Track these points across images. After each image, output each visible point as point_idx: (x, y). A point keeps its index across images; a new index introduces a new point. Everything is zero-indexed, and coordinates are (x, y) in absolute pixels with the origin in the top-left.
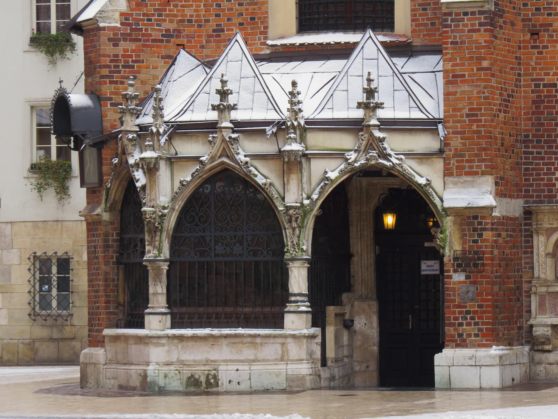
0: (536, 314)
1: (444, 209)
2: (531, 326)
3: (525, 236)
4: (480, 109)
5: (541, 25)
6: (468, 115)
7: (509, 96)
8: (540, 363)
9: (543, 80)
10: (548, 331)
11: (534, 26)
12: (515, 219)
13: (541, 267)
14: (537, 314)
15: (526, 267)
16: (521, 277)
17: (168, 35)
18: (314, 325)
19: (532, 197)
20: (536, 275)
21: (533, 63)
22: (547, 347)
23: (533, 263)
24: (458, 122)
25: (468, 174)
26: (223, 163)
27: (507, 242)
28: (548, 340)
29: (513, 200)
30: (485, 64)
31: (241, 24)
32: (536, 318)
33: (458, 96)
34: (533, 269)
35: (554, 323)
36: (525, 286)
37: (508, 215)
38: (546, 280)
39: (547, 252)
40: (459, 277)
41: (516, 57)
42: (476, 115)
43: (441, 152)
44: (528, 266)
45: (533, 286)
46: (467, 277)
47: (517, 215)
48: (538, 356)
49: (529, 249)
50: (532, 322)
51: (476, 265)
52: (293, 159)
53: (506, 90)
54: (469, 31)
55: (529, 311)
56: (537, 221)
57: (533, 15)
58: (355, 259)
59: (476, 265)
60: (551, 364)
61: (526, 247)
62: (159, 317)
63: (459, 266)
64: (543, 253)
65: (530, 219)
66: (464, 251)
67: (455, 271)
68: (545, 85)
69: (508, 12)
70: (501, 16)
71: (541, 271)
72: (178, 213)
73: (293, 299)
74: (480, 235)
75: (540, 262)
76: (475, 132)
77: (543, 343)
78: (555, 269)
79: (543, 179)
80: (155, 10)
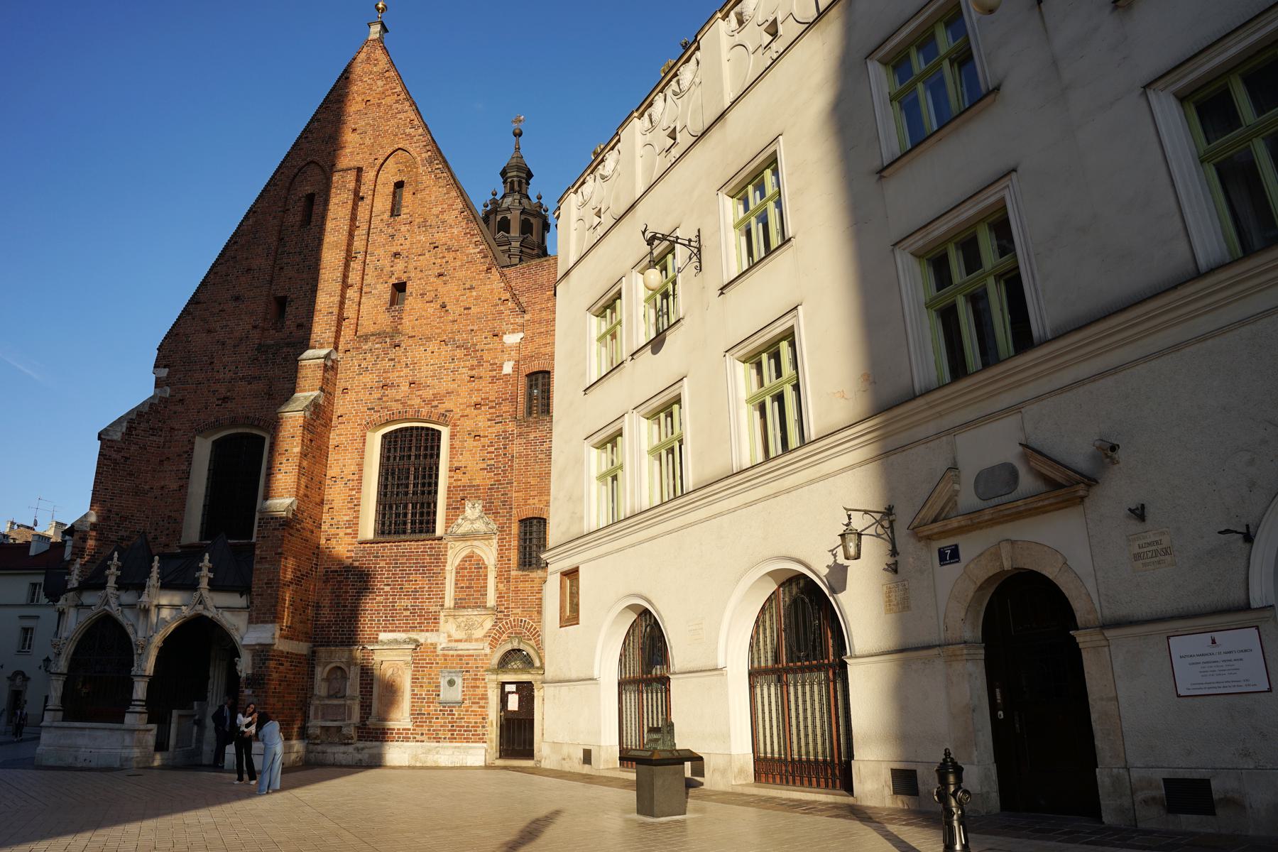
1: (245, 646)
2: (308, 727)
4: (274, 580)
5: (333, 535)
6: (266, 584)
7: (302, 575)
8: (312, 752)
9: (331, 568)
10: (318, 732)
11: (328, 535)
12: (302, 655)
16: (306, 694)
17: (122, 539)
18: (150, 722)
19: (317, 642)
20: (315, 693)
21: (325, 558)
22: (319, 741)
24: (260, 588)
25: (263, 622)
26: (105, 610)
27: (292, 670)
28: (317, 737)
29: (301, 643)
30: (280, 550)
31: (167, 535)
33: (262, 571)
35: (322, 725)
36: (308, 700)
37: (293, 652)
38: (320, 697)
40: (248, 692)
41: (314, 553)
42: (271, 583)
43: (248, 607)
46: (253, 693)
47: (305, 653)
48: (311, 747)
49: (311, 675)
50: (309, 724)
51: (260, 684)
52: (142, 606)
53: (300, 571)
54: (274, 529)
55: (309, 717)
57: (328, 528)
58: (211, 681)
59: (260, 684)
60: (319, 753)
61: (311, 675)
62: (52, 713)
63: (249, 684)
66: (253, 674)
67: (246, 688)
68: (331, 572)
69: (308, 523)
70: (300, 524)
72: (76, 643)
73: (133, 703)
74: (264, 664)
76: (270, 594)
77: (315, 738)
79: (325, 631)
80: (115, 523)
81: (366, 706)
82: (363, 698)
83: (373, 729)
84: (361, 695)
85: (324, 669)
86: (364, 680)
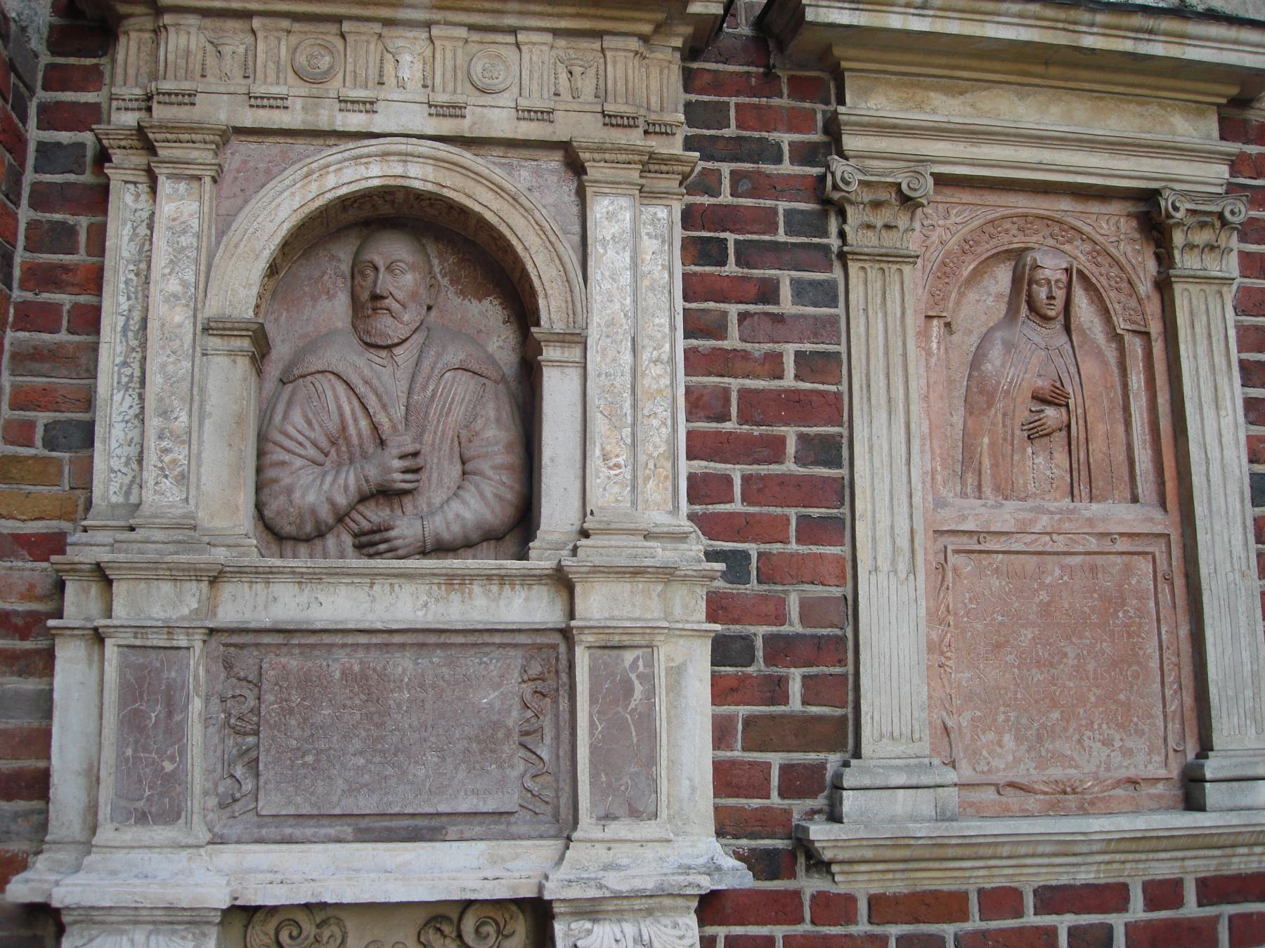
0: (92, 808)
3: (41, 198)
13: (154, 423)
14: (104, 811)
15: (31, 425)
23: (88, 401)
32: (87, 846)
34: (90, 443)
39: (213, 308)
44: (43, 418)
45: (74, 569)
56: (154, 76)
64: (180, 316)
65: (92, 78)
71: (151, 458)
75: (155, 381)
78: (261, 454)
81: (780, 649)
82: (736, 565)
83: (881, 907)
84: (707, 525)
85: (223, 224)
86: (723, 362)
